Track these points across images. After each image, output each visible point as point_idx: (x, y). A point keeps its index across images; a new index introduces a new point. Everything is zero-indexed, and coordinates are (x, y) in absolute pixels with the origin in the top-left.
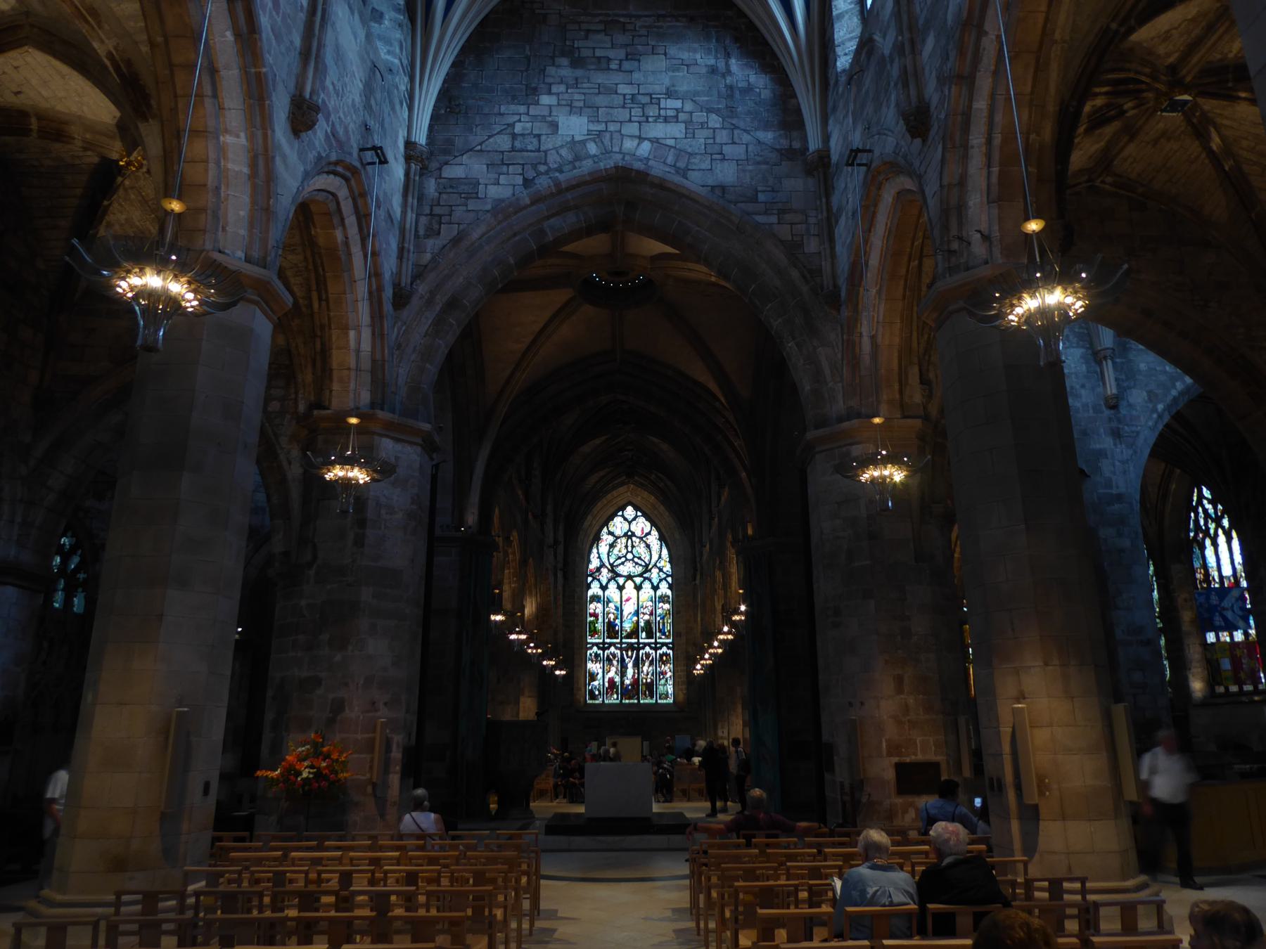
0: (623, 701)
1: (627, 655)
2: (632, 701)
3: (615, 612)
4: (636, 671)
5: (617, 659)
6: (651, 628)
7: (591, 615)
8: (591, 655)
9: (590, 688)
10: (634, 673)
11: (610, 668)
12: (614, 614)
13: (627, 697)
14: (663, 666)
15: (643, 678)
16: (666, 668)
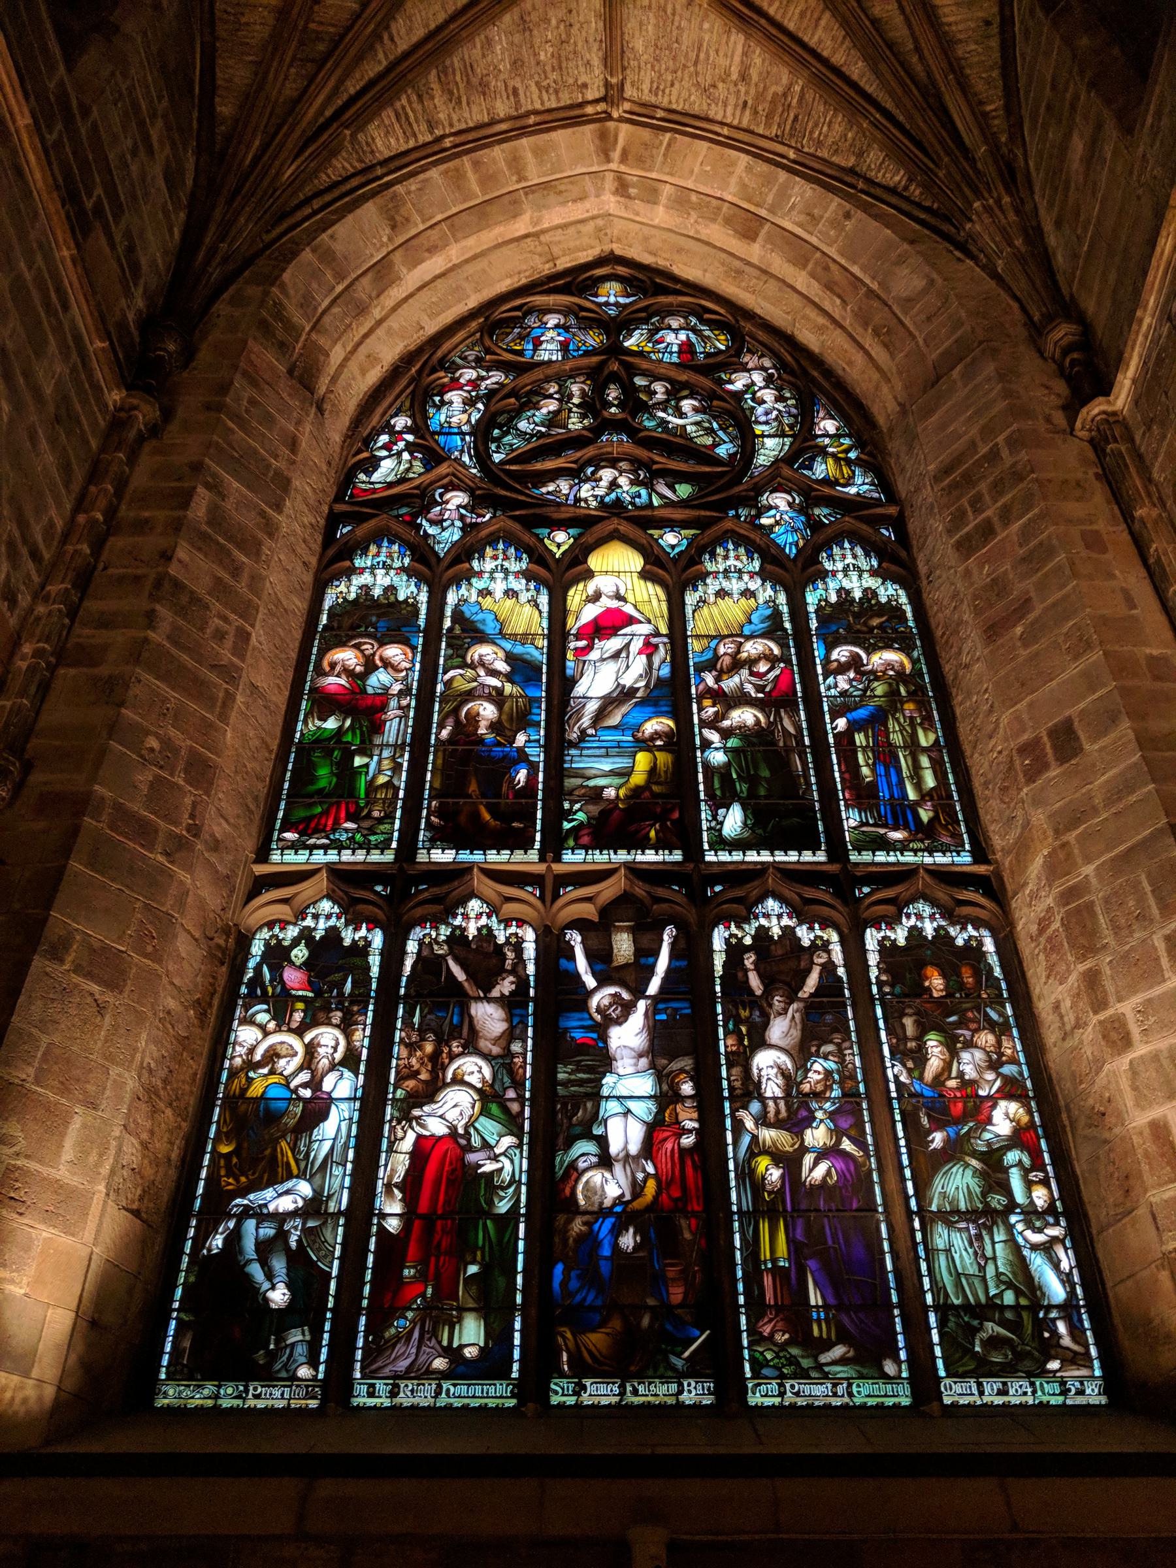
0: (561, 1394)
1: (600, 957)
2: (657, 1392)
3: (508, 688)
4: (687, 1088)
5: (506, 986)
6: (788, 783)
7: (325, 704)
8: (277, 955)
9: (218, 1242)
10: (666, 1098)
11: (437, 1063)
12: (497, 697)
13: (596, 1340)
14: (934, 1046)
15: (756, 1149)
16: (969, 1063)
